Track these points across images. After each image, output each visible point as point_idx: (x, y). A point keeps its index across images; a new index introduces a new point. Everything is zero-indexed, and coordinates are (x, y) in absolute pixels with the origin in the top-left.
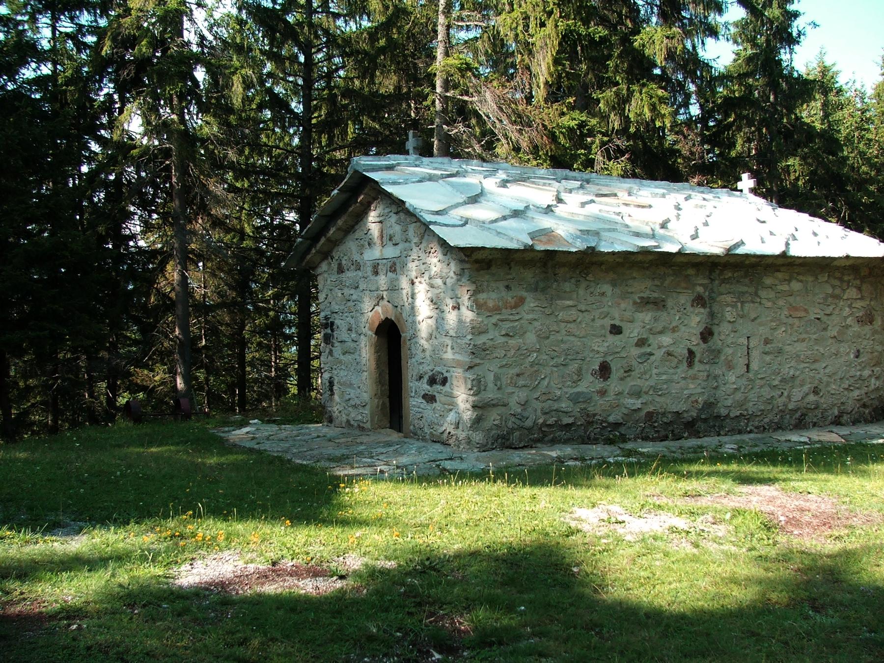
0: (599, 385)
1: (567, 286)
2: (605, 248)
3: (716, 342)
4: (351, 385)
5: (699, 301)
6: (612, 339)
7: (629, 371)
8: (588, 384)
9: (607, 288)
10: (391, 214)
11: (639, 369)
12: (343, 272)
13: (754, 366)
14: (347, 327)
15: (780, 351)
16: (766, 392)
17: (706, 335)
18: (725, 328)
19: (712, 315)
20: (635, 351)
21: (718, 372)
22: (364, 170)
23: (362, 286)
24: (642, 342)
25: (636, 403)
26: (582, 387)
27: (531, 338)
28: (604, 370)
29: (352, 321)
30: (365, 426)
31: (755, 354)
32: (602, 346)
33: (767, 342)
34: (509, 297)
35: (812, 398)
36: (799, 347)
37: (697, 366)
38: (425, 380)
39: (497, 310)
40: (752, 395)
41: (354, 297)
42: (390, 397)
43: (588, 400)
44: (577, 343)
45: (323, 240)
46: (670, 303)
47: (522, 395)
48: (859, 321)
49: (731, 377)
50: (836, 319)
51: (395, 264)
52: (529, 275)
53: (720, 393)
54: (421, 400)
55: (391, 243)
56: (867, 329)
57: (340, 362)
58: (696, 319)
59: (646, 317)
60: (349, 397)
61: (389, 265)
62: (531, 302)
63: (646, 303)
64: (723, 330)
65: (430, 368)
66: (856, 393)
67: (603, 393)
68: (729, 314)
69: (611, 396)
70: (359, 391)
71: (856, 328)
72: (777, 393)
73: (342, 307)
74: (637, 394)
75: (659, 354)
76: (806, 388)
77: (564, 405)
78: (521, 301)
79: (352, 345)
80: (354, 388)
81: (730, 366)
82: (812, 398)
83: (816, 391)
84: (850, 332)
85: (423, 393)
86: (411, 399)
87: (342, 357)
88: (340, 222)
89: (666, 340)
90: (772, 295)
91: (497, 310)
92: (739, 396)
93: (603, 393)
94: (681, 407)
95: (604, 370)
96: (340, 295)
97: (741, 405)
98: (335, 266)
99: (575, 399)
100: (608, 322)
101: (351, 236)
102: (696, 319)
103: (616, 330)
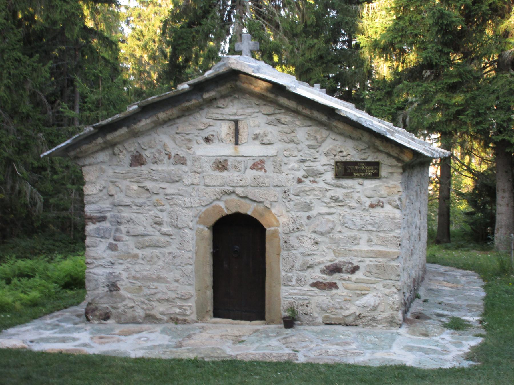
4: (159, 279)
10: (260, 114)
12: (142, 164)
14: (150, 221)
22: (253, 72)
23: (187, 180)
29: (165, 217)
30: (187, 318)
38: (317, 269)
41: (169, 191)
42: (214, 288)
45: (123, 130)
51: (263, 162)
54: (307, 288)
55: (257, 142)
57: (136, 256)
60: (155, 291)
61: (250, 163)
65: (329, 258)
70: (176, 284)
73: (142, 201)
79: (163, 239)
80: (167, 282)
85: (312, 281)
86: (283, 288)
87: (136, 251)
88: (162, 115)
96: (135, 187)
98: (126, 158)
101: (166, 129)
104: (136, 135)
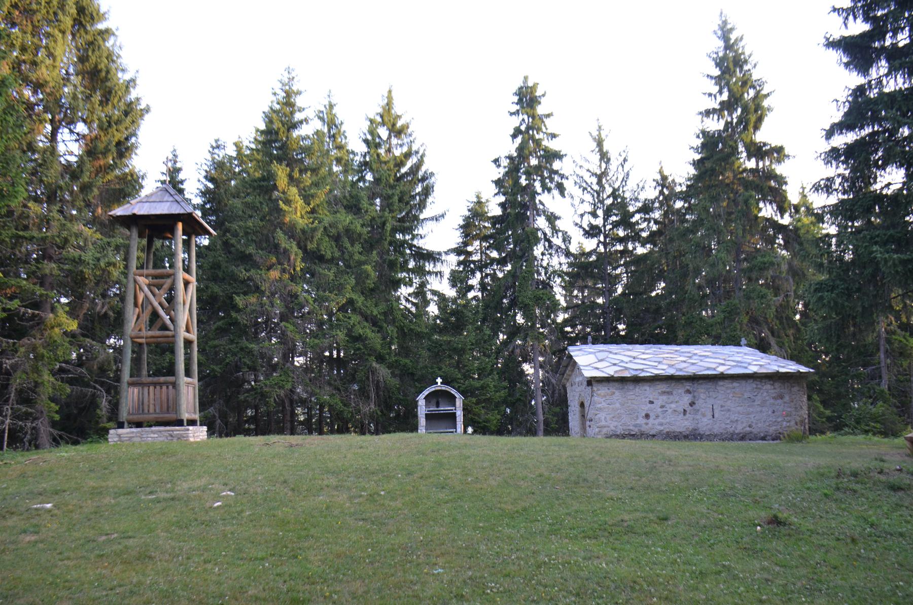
0: (645, 421)
1: (631, 388)
2: (643, 374)
3: (696, 407)
5: (688, 392)
6: (649, 405)
7: (657, 417)
8: (641, 421)
9: (648, 388)
11: (661, 416)
13: (716, 416)
15: (729, 410)
16: (723, 426)
17: (692, 404)
18: (701, 401)
19: (694, 397)
20: (660, 410)
21: (698, 417)
24: (662, 407)
25: (662, 428)
26: (638, 422)
27: (618, 405)
28: (647, 416)
31: (715, 411)
32: (647, 408)
33: (722, 406)
34: (609, 392)
35: (748, 429)
36: (739, 408)
37: (688, 415)
39: (605, 396)
40: (715, 426)
43: (641, 426)
44: (636, 407)
46: (674, 392)
47: (616, 424)
48: (774, 398)
49: (705, 420)
50: (759, 397)
52: (616, 384)
53: (699, 426)
56: (780, 401)
58: (687, 399)
59: (665, 397)
62: (617, 393)
63: (664, 393)
64: (700, 403)
66: (774, 428)
67: (647, 424)
68: (702, 396)
69: (650, 425)
71: (772, 401)
72: (728, 426)
74: (661, 424)
75: (670, 411)
76: (744, 425)
77: (631, 428)
78: (614, 393)
81: (704, 415)
82: (748, 429)
83: (750, 426)
84: (768, 403)
89: (673, 406)
90: (723, 388)
91: (605, 396)
92: (709, 426)
93: (647, 424)
94: (681, 430)
95: (647, 416)
97: (710, 430)
99: (635, 426)
100: (648, 400)
102: (687, 399)
103: (651, 402)
104: (570, 375)
